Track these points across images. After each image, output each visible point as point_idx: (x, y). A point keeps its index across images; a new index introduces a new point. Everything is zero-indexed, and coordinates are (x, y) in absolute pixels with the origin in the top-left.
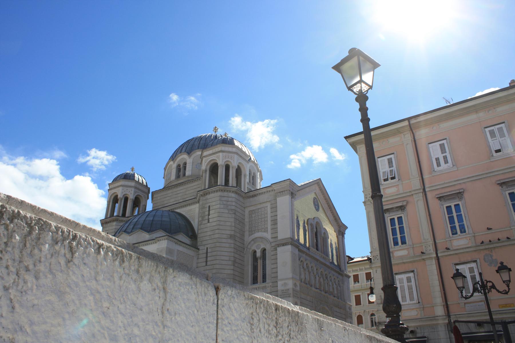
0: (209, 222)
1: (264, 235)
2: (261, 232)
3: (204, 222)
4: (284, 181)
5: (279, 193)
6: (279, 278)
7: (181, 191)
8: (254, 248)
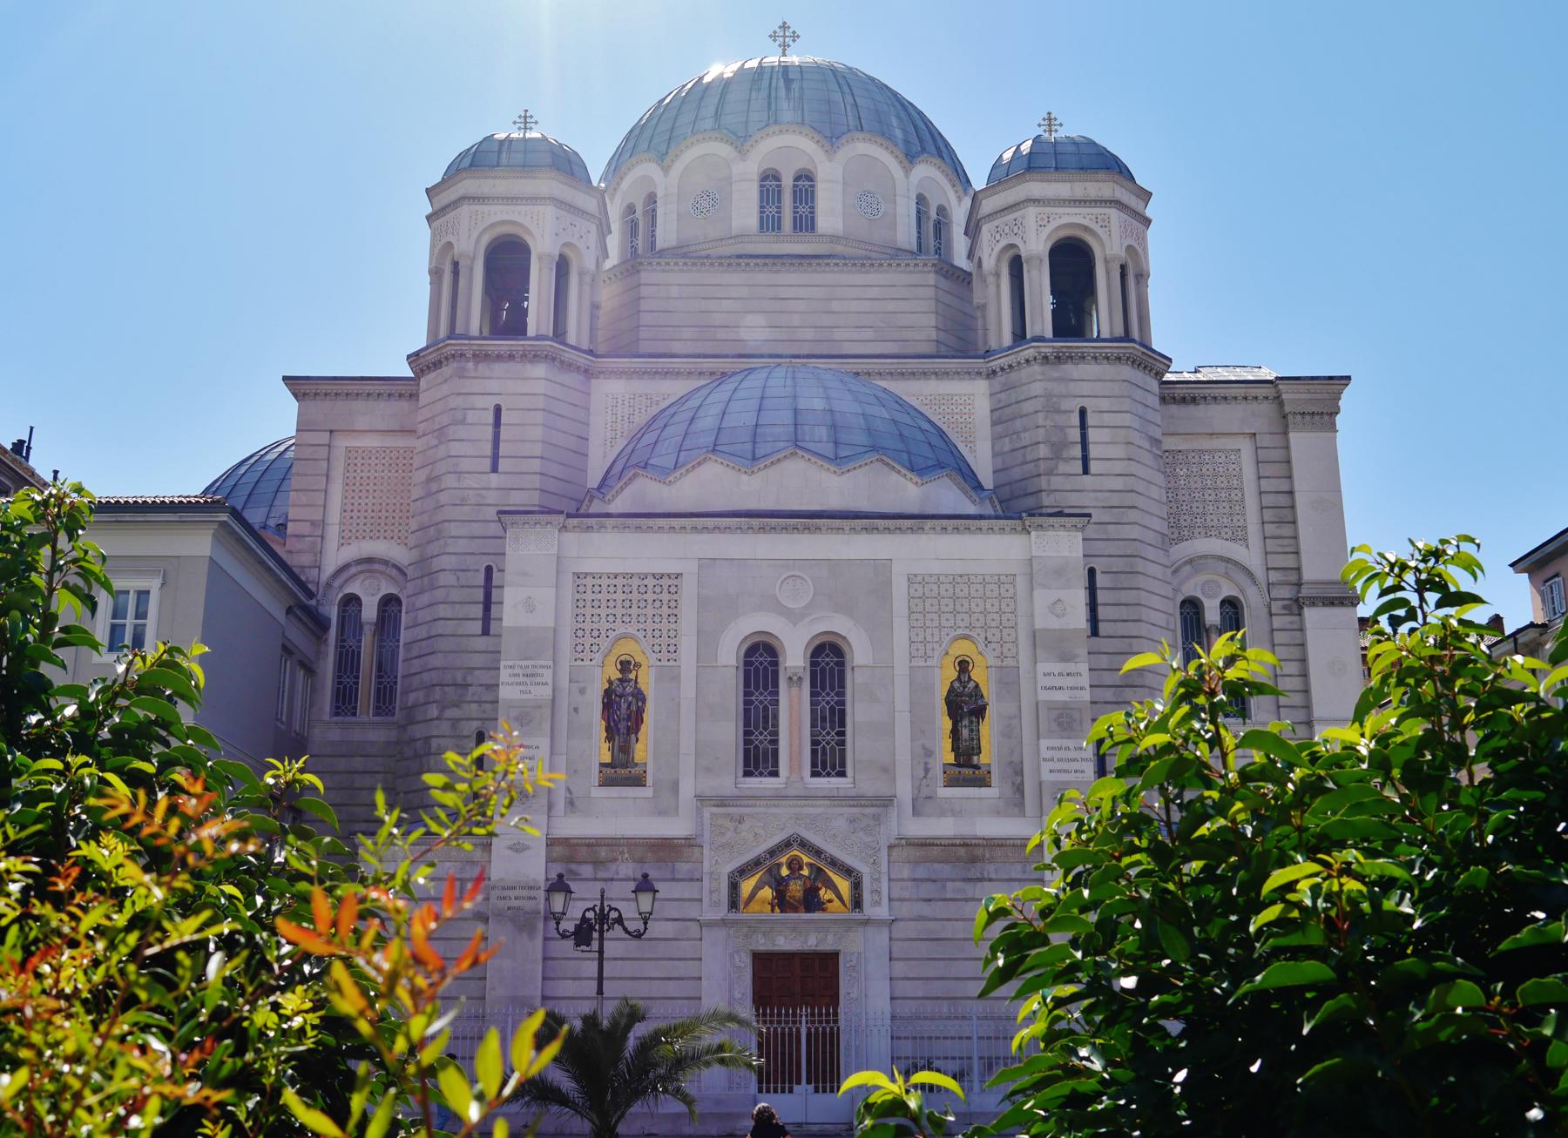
0: (1086, 471)
1: (1235, 551)
2: (1219, 535)
3: (1063, 467)
4: (1331, 378)
5: (1299, 417)
6: (1318, 712)
7: (802, 292)
8: (1191, 589)
